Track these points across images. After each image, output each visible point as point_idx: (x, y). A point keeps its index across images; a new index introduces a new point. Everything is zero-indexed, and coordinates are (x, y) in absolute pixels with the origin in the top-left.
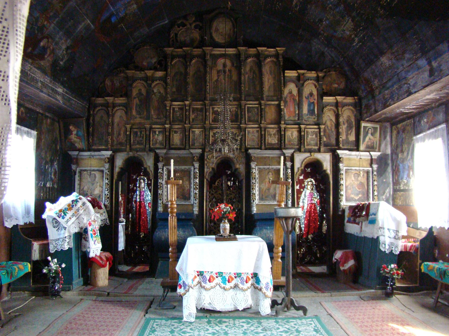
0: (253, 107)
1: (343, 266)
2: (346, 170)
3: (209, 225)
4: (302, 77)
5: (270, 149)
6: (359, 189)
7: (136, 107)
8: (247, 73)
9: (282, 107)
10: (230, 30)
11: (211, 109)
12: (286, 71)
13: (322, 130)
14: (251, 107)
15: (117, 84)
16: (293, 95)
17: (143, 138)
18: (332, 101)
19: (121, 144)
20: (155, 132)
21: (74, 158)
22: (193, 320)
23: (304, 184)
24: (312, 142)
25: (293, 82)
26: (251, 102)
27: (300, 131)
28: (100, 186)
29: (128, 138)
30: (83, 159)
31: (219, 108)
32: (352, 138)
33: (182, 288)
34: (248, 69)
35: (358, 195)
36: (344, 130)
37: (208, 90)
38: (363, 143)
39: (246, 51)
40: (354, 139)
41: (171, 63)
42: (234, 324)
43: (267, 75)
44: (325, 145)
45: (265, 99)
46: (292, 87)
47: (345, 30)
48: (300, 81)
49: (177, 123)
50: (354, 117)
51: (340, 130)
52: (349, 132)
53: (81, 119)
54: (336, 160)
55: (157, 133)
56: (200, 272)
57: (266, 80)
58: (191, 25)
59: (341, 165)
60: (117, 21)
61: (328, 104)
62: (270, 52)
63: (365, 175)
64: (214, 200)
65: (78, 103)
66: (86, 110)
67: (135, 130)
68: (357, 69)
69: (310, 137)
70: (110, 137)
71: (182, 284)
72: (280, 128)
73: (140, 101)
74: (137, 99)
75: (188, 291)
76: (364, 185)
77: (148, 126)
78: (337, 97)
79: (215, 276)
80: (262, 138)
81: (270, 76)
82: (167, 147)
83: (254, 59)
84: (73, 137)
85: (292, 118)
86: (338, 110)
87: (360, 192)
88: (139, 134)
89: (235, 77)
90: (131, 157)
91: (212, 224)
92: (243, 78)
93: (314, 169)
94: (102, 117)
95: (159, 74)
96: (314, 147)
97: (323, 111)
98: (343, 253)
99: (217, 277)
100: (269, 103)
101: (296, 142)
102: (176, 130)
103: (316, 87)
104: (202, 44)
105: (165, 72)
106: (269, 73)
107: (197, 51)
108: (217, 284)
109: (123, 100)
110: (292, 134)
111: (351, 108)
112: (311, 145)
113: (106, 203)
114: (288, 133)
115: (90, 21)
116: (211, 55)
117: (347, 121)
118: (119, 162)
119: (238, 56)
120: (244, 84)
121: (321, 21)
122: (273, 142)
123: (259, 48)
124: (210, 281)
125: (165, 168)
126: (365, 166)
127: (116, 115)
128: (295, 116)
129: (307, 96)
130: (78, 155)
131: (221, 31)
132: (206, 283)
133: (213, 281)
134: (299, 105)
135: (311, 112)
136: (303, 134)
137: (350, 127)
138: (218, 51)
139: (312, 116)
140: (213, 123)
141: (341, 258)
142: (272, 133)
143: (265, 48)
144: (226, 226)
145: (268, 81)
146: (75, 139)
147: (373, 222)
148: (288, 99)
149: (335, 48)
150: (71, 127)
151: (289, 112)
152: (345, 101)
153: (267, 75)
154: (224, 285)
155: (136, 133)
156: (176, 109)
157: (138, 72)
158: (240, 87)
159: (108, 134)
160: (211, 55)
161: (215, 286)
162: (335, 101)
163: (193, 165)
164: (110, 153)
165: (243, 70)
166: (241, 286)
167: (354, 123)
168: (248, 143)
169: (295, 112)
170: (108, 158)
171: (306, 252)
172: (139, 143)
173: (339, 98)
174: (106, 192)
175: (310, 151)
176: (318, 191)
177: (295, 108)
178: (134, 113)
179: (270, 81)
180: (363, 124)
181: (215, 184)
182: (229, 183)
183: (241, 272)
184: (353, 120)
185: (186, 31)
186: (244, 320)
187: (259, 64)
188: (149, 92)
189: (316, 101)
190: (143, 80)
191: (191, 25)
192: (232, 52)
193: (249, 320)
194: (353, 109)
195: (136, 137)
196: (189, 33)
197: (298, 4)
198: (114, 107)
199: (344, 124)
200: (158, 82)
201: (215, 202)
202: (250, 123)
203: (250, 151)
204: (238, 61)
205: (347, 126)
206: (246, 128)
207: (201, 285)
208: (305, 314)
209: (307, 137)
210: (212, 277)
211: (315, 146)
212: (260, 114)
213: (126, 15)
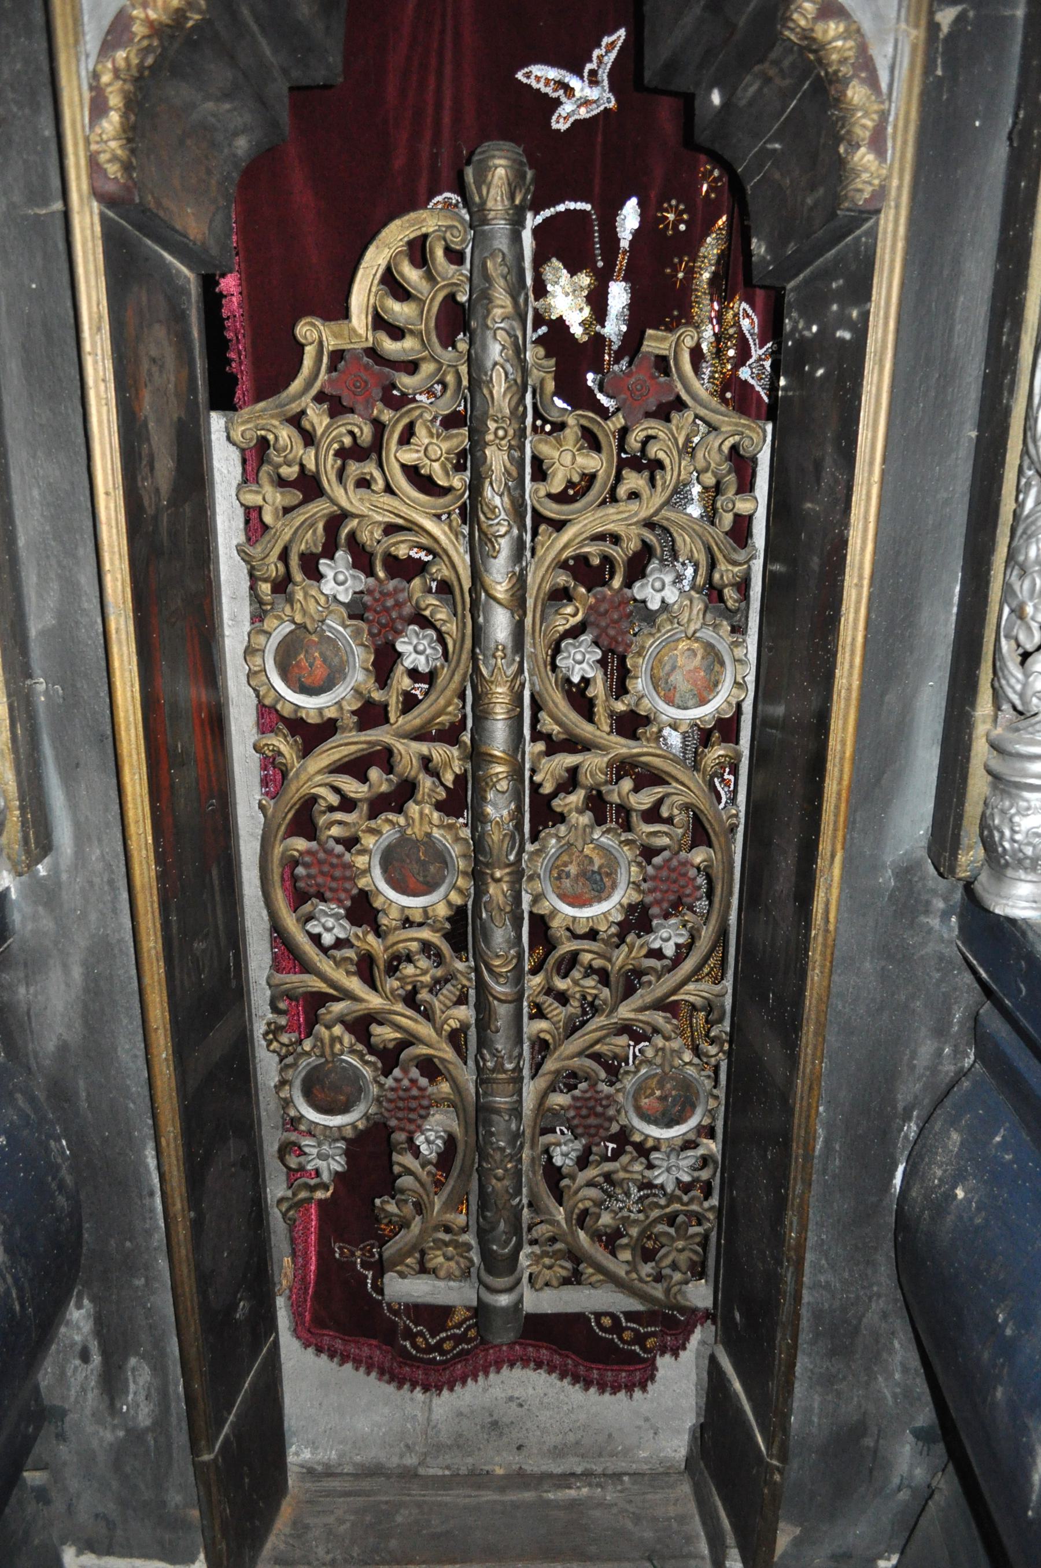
3: (278, 932)
91: (331, 923)
181: (338, 310)
182: (566, 300)
201: (356, 610)
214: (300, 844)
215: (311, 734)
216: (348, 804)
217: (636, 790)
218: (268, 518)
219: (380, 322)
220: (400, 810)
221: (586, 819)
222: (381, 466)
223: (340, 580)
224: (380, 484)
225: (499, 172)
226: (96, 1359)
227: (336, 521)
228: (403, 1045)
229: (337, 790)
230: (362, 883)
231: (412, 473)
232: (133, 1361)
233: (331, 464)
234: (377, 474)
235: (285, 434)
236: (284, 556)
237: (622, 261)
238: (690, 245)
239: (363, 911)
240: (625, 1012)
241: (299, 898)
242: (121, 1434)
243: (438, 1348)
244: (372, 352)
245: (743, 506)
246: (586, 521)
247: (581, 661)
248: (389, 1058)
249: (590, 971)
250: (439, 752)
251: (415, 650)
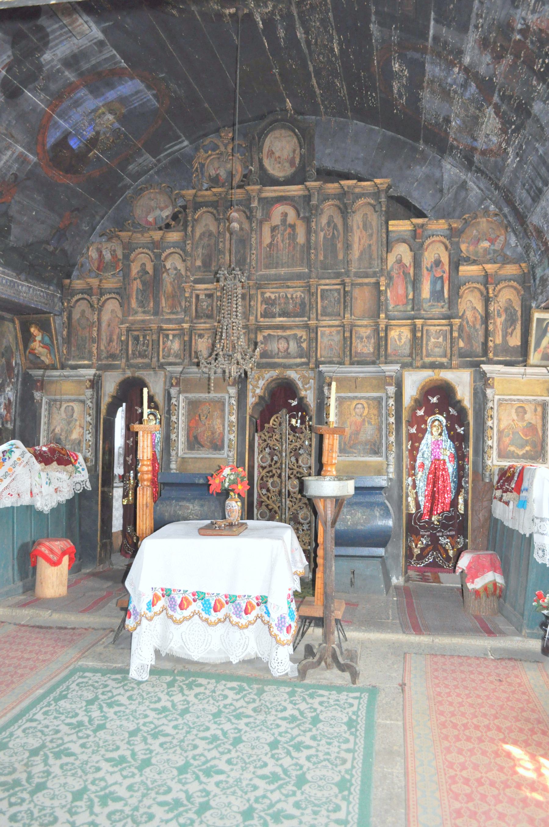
0: (331, 290)
1: (473, 582)
2: (499, 399)
4: (419, 231)
5: (359, 363)
6: (526, 435)
7: (137, 294)
8: (322, 230)
9: (382, 288)
10: (294, 151)
11: (259, 296)
12: (391, 222)
13: (455, 328)
14: (327, 290)
15: (108, 256)
16: (404, 266)
17: (148, 347)
18: (476, 273)
19: (113, 356)
20: (167, 336)
21: (38, 381)
22: (145, 676)
23: (426, 424)
24: (437, 350)
25: (404, 241)
26: (327, 281)
27: (414, 330)
28: (80, 426)
29: (124, 347)
30: (52, 382)
31: (272, 293)
32: (515, 341)
33: (132, 617)
34: (324, 221)
35: (522, 447)
36: (500, 327)
37: (253, 263)
38: (535, 350)
39: (320, 188)
40: (519, 344)
41: (193, 217)
42: (214, 691)
43: (359, 231)
44: (462, 355)
45: (352, 275)
46: (402, 252)
47: (488, 135)
48: (417, 242)
49: (202, 321)
50: (520, 303)
51: (491, 327)
52: (510, 330)
53: (47, 315)
54: (482, 381)
55: (171, 337)
56: (167, 590)
57: (356, 239)
58: (226, 146)
59: (489, 392)
60: (81, 145)
61: (469, 280)
62: (363, 188)
63: (539, 409)
64: (268, 450)
65: (34, 289)
66: (56, 300)
67: (136, 333)
68: (521, 210)
69: (433, 340)
70: (96, 345)
71: (131, 611)
72: (377, 325)
73: (144, 283)
74: (138, 280)
75: (139, 624)
76: (536, 429)
77: (154, 326)
78: (484, 265)
79: (191, 598)
80: (347, 342)
81: (364, 232)
82: (186, 361)
83: (337, 202)
84: (37, 346)
85: (401, 308)
86: (487, 289)
87: (527, 441)
88: (141, 339)
89: (301, 239)
90: (129, 378)
91: (264, 491)
92: (313, 238)
93: (441, 397)
94: (83, 312)
95: (174, 236)
96: (439, 359)
97: (458, 294)
98: (473, 558)
99: (195, 601)
100: (360, 280)
101: (407, 350)
102: (202, 332)
103: (446, 248)
104: (246, 179)
105: (182, 234)
106: (361, 226)
107: (238, 194)
108: (194, 613)
109: (116, 283)
110: (400, 336)
111: (515, 284)
112: (435, 356)
113: (88, 455)
114: (393, 334)
115: (23, 147)
116: (261, 200)
117: (506, 310)
118: (110, 386)
119: (307, 198)
120: (315, 249)
121: (447, 120)
122: (366, 351)
123: (342, 182)
124: (181, 607)
125: (181, 397)
126: (539, 393)
127: (104, 309)
128: (407, 304)
129: (429, 266)
130: (43, 376)
131: (277, 154)
132: (174, 610)
133: (188, 607)
134: (416, 284)
135: (437, 295)
136: (419, 334)
137: (511, 321)
138: (270, 192)
139: (438, 302)
140: (262, 319)
141: (469, 567)
142: (365, 335)
143: (355, 182)
144: (234, 506)
145: (359, 240)
146: (41, 349)
147: (523, 504)
148: (394, 273)
149: (483, 173)
150: (32, 330)
151: (395, 295)
152: (502, 272)
153: (359, 231)
154: (207, 616)
155: (136, 339)
156: (200, 297)
157: (139, 235)
158: (309, 254)
159: (93, 340)
160: (261, 200)
161: (191, 617)
162: (483, 273)
163: (228, 392)
164: (92, 371)
165: (313, 224)
166: (235, 619)
167: (519, 313)
168: (322, 353)
169: (407, 296)
170: (90, 381)
171: (427, 545)
172: (142, 355)
173: (490, 268)
174: (88, 437)
175: (433, 366)
176: (451, 438)
177: (407, 288)
178: (134, 304)
179: (362, 241)
180: (537, 315)
182: (293, 421)
183: (237, 594)
184: (518, 308)
185: (219, 158)
186: (234, 684)
187: (345, 211)
188: (159, 269)
189: (446, 276)
190: (148, 248)
191: (226, 146)
192: (296, 193)
193: (245, 685)
194: (519, 288)
195: (137, 345)
196: (219, 160)
197: (403, 90)
198: (102, 294)
199: (499, 315)
200: (172, 250)
201: (269, 454)
202: (324, 318)
203: (322, 368)
204: (307, 208)
205: (506, 320)
206: (317, 328)
207: (167, 614)
208: (354, 682)
209: (428, 340)
210: (187, 600)
211: (441, 356)
212: (342, 300)
213: (98, 133)
215: (264, 468)
223: (268, 450)
225: (284, 411)
239: (268, 490)
240: (300, 504)
241: (261, 488)
247: (293, 459)
251: (275, 458)
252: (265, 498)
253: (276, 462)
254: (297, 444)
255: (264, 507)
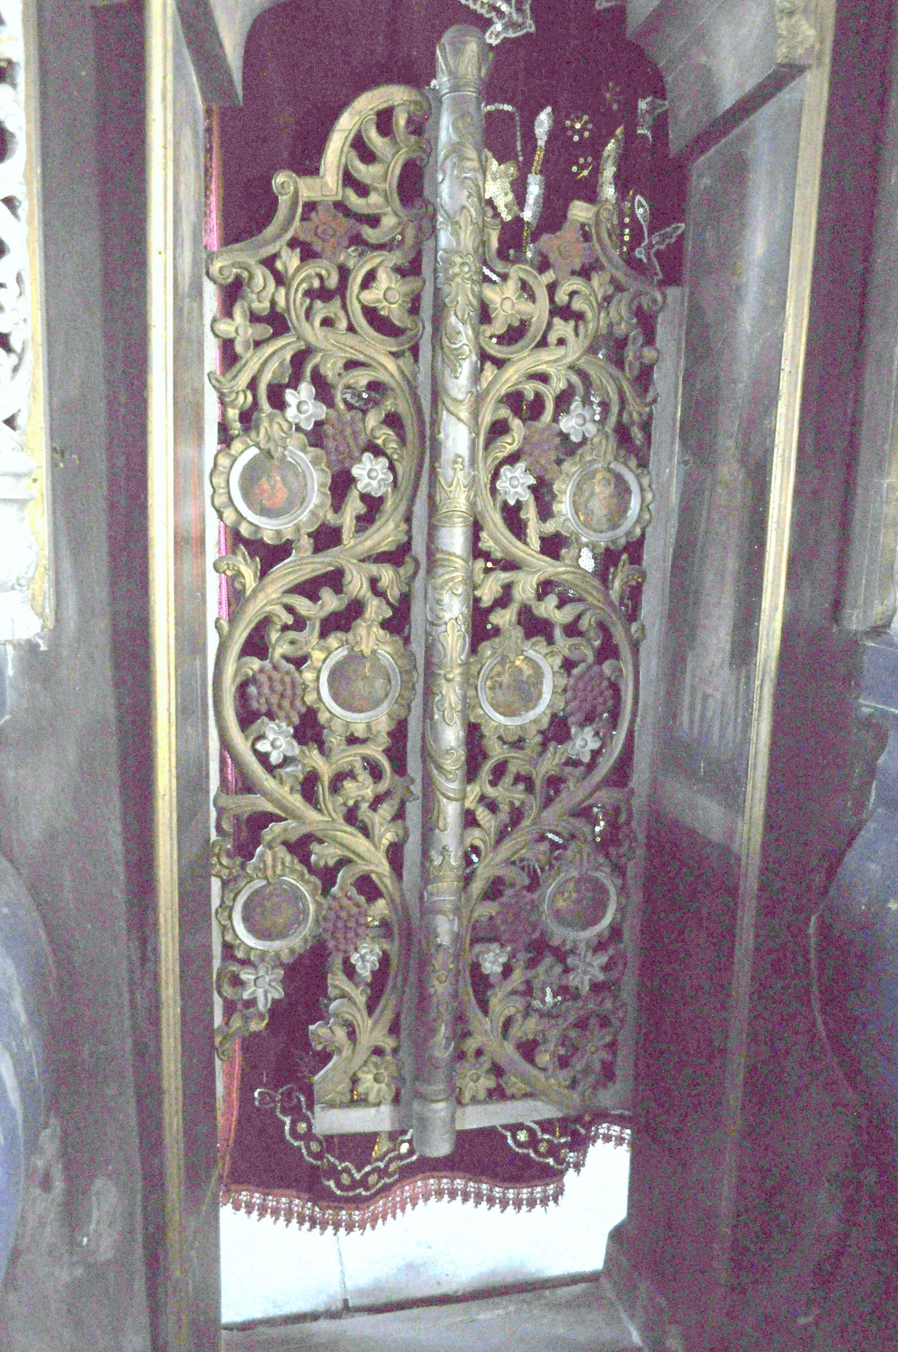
91: (278, 739)
201: (316, 436)
214: (255, 663)
215: (270, 555)
216: (300, 624)
217: (559, 607)
218: (239, 348)
219: (349, 179)
220: (346, 629)
221: (519, 632)
222: (344, 307)
224: (344, 324)
226: (59, 1185)
227: (299, 359)
228: (343, 862)
229: (290, 609)
230: (310, 698)
231: (371, 314)
232: (99, 1183)
233: (299, 301)
234: (341, 314)
235: (261, 276)
236: (253, 385)
237: (539, 156)
238: (594, 147)
239: (309, 729)
241: (247, 718)
242: (79, 1272)
243: (363, 1183)
244: (340, 206)
245: (649, 354)
246: (524, 360)
248: (328, 876)
249: (518, 779)
250: (386, 574)
251: (370, 474)
252: (282, 792)
253: (373, 504)
254: (544, 360)
255: (270, 855)
